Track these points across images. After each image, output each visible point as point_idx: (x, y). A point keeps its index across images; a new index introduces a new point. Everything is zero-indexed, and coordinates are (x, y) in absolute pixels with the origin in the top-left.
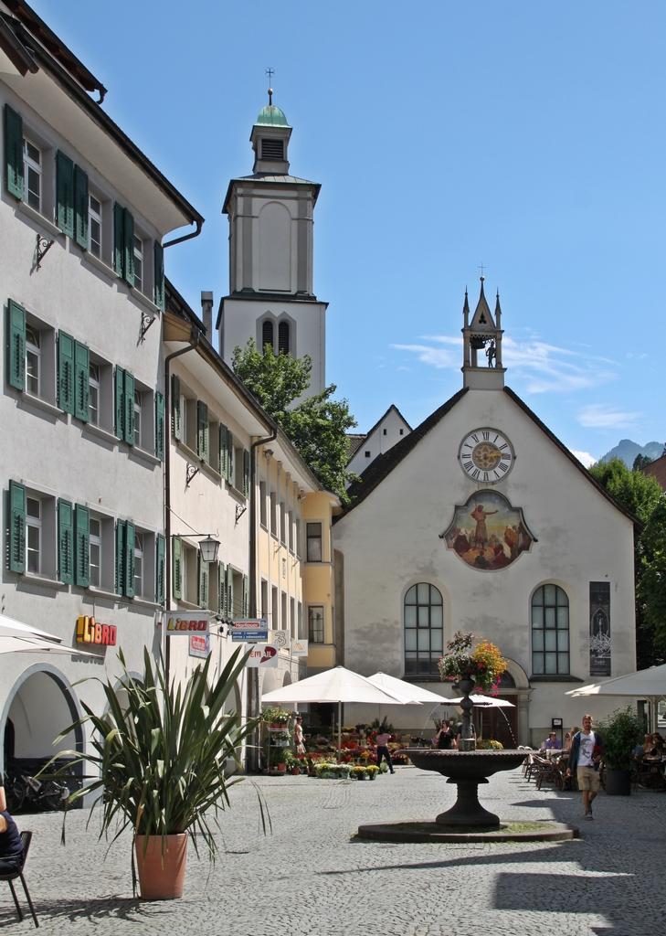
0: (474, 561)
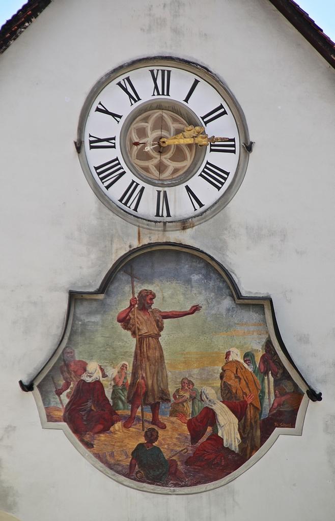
0: (126, 461)
